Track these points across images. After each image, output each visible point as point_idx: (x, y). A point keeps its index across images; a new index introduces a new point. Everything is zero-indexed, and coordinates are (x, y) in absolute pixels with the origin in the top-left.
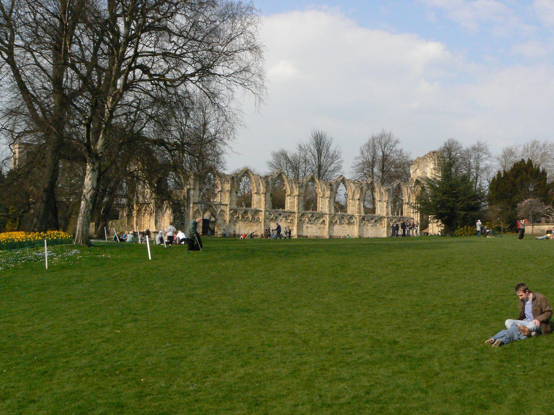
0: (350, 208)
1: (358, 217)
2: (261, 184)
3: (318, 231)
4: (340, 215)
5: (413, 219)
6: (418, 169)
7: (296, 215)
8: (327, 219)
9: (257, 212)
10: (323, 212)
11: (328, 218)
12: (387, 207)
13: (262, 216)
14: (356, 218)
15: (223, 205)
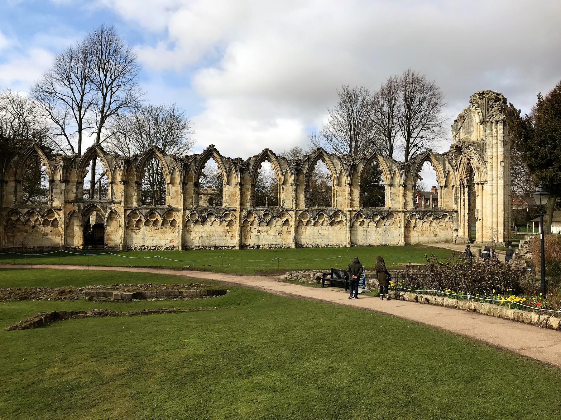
0: (336, 199)
1: (348, 213)
2: (177, 169)
3: (278, 237)
4: (316, 210)
5: (457, 212)
6: (462, 129)
7: (238, 214)
8: (292, 218)
9: (171, 211)
10: (286, 208)
11: (293, 216)
12: (404, 195)
13: (178, 217)
14: (346, 215)
15: (114, 203)
